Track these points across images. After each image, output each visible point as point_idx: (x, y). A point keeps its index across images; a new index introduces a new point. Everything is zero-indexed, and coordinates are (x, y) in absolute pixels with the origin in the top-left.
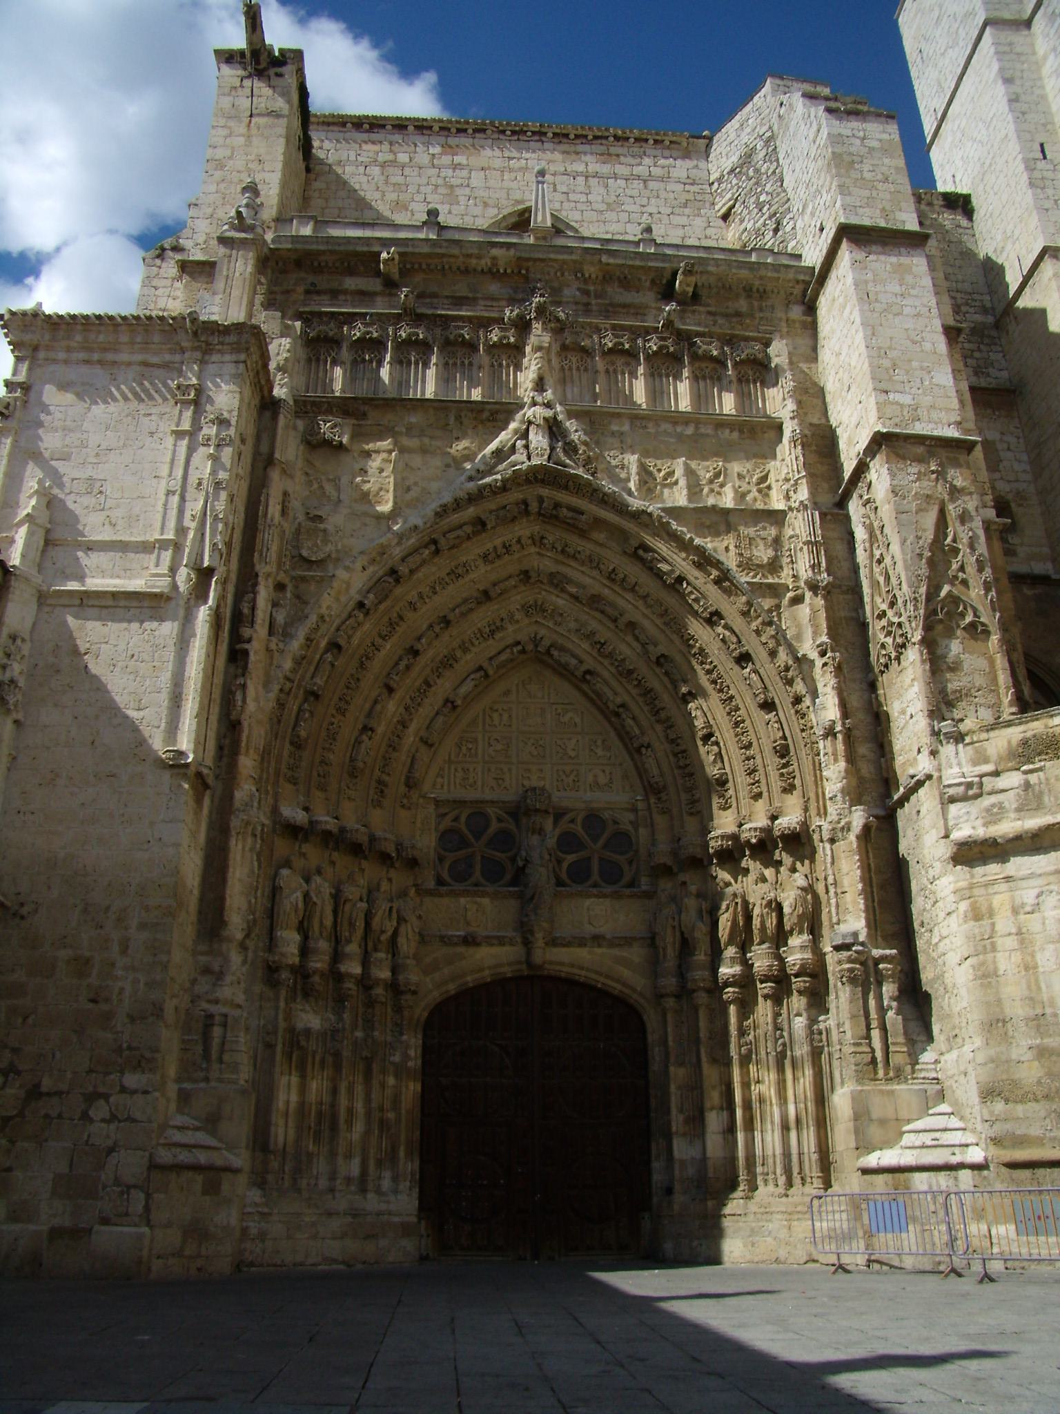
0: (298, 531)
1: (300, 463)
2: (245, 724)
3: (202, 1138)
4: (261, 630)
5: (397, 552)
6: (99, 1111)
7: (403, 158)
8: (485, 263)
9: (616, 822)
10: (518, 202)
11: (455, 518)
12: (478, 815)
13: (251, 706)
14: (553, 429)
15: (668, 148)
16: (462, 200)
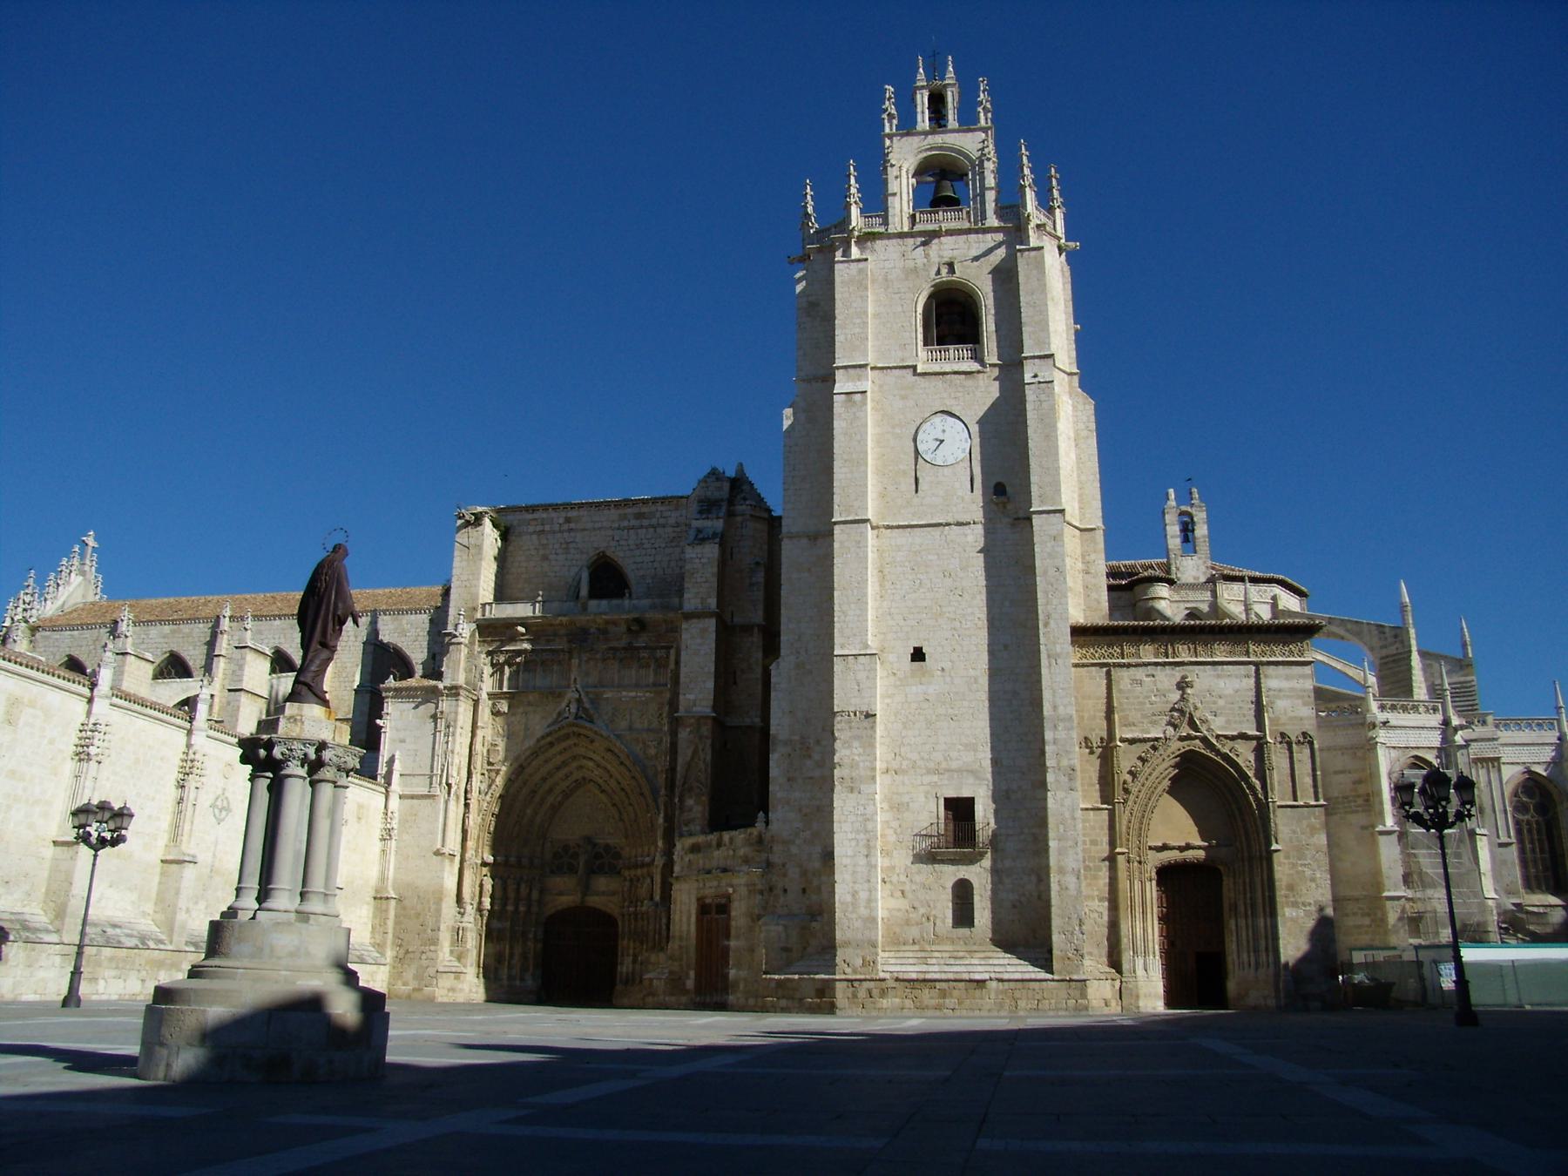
0: (488, 751)
1: (491, 721)
2: (469, 830)
3: (457, 964)
4: (474, 795)
5: (523, 757)
6: (424, 957)
7: (547, 528)
8: (558, 622)
9: (615, 848)
10: (596, 549)
11: (543, 742)
12: (566, 848)
13: (471, 823)
14: (579, 701)
15: (669, 505)
16: (572, 551)
